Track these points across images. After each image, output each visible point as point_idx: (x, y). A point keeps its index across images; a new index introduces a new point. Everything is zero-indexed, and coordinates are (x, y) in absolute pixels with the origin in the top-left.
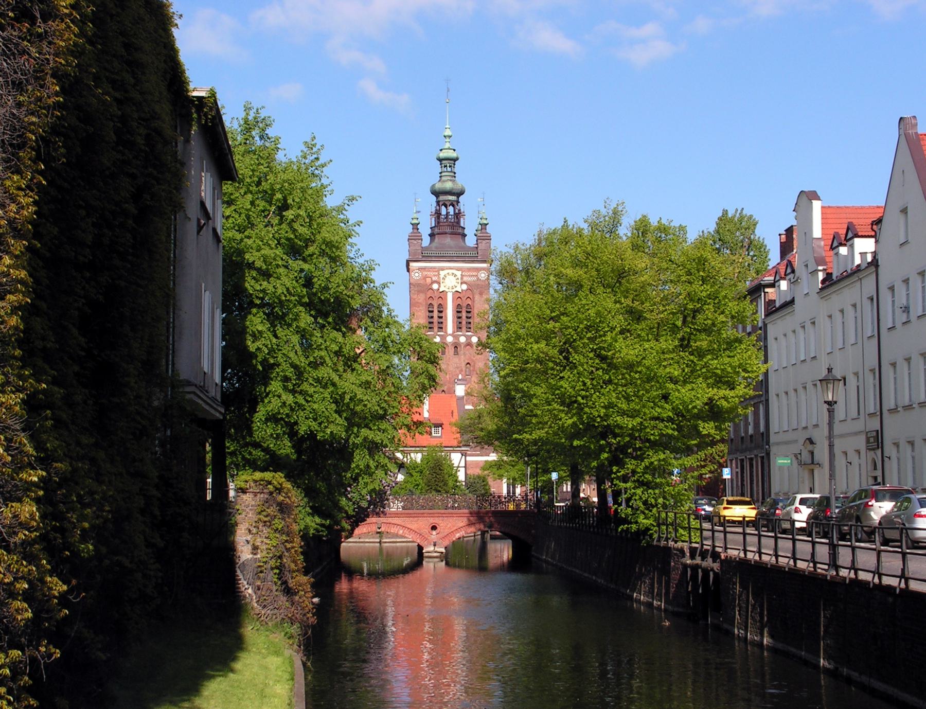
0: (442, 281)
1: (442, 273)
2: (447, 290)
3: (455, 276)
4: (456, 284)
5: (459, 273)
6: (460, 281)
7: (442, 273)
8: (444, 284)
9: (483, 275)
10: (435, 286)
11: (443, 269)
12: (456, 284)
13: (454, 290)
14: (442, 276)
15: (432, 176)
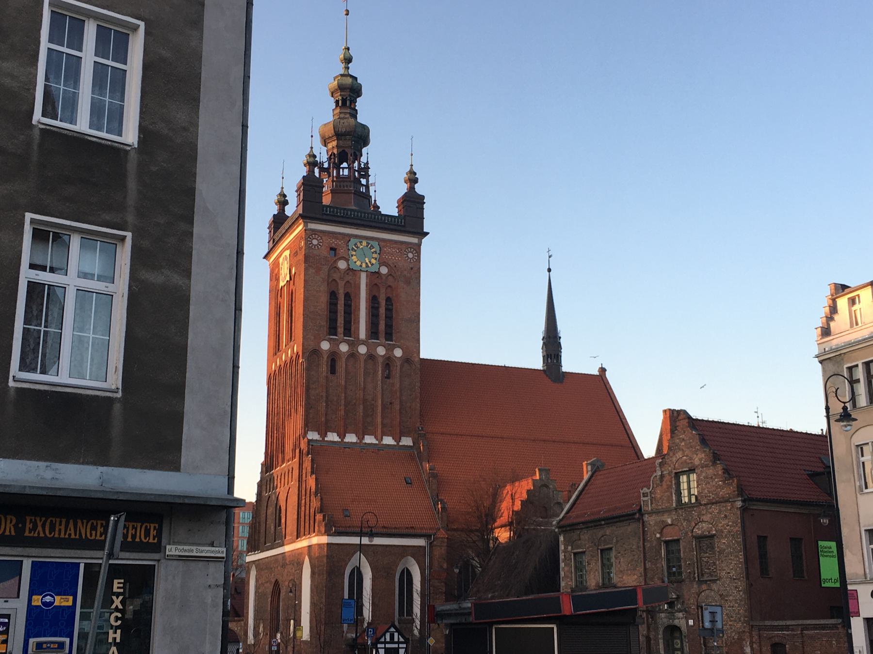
4: (373, 261)
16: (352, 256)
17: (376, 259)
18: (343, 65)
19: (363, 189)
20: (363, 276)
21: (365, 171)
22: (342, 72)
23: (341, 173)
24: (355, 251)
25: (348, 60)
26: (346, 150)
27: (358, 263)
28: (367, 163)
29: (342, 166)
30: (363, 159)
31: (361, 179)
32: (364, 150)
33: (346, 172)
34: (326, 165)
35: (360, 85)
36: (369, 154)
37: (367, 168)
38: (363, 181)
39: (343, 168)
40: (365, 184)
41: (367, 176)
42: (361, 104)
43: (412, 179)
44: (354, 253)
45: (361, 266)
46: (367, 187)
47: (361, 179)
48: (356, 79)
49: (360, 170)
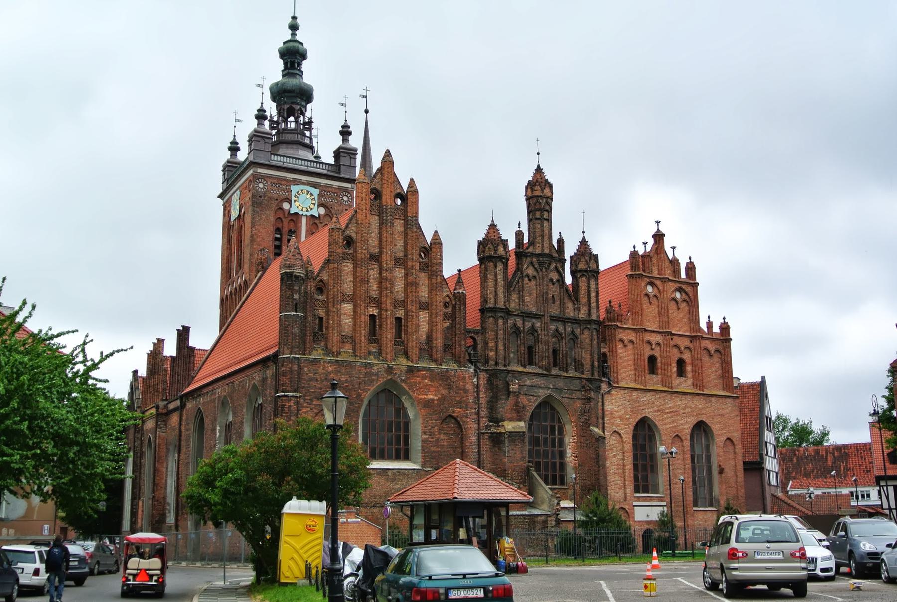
0: (293, 199)
1: (295, 189)
2: (301, 213)
3: (312, 195)
4: (312, 206)
5: (316, 192)
6: (316, 202)
7: (295, 189)
8: (297, 204)
9: (345, 199)
10: (286, 206)
11: (296, 182)
12: (312, 206)
13: (309, 214)
14: (294, 193)
15: (275, 71)
16: (295, 202)
17: (315, 204)
18: (290, 32)
19: (307, 141)
20: (304, 220)
21: (309, 124)
22: (288, 37)
23: (289, 126)
24: (298, 198)
25: (294, 28)
26: (294, 106)
27: (300, 208)
28: (311, 118)
29: (289, 119)
30: (308, 114)
31: (306, 132)
32: (309, 106)
33: (293, 125)
34: (275, 119)
35: (306, 51)
36: (313, 110)
37: (310, 122)
38: (308, 133)
39: (290, 122)
40: (309, 135)
41: (310, 129)
42: (306, 66)
43: (345, 132)
44: (296, 199)
45: (302, 210)
46: (311, 138)
47: (306, 132)
48: (302, 44)
49: (305, 123)
